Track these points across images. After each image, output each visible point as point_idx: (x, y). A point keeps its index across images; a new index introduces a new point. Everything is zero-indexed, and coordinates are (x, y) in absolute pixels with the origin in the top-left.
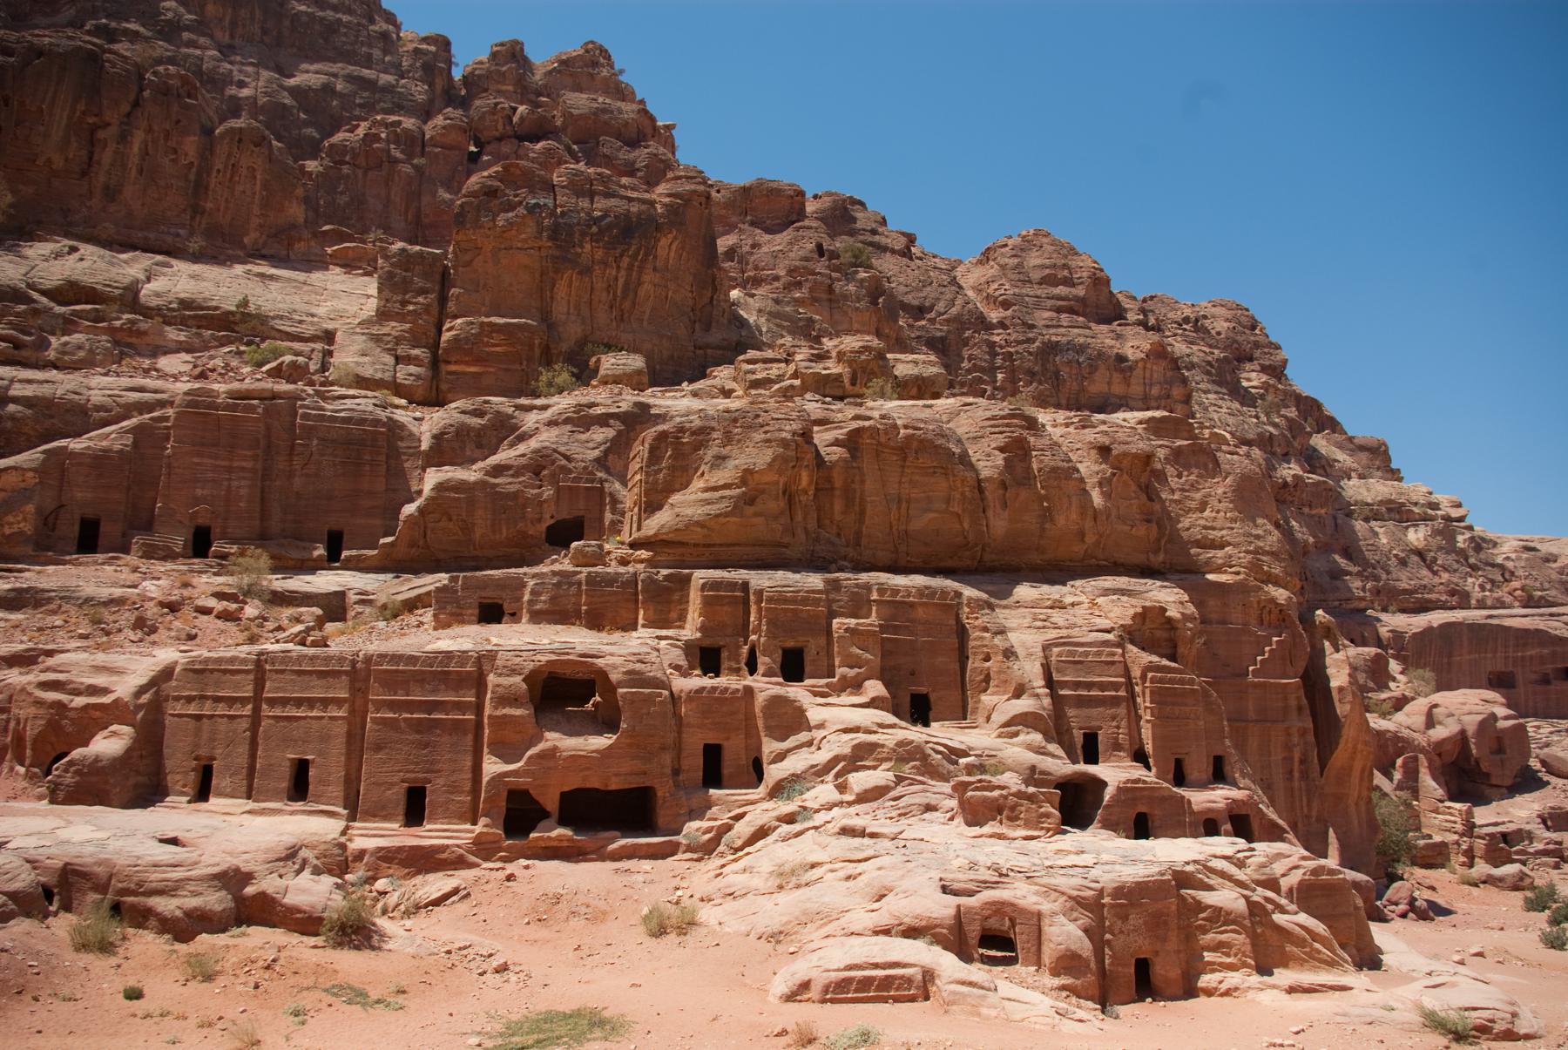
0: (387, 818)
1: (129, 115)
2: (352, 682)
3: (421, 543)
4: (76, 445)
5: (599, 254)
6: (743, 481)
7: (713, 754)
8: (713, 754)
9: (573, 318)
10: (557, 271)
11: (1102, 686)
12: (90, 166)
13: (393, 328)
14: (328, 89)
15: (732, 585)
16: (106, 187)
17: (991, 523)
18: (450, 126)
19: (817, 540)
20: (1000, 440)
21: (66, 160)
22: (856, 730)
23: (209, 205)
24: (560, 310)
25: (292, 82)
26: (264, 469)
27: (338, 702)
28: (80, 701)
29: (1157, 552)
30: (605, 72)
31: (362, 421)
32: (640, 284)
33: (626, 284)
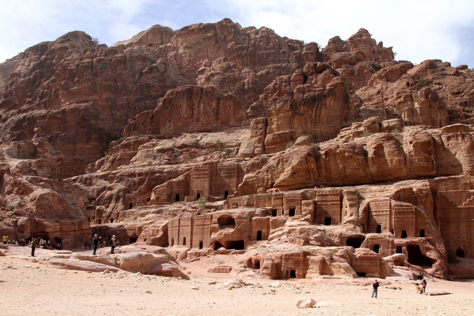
7: (259, 233)
8: (259, 233)
9: (300, 128)
13: (254, 140)
22: (292, 226)
31: (231, 166)
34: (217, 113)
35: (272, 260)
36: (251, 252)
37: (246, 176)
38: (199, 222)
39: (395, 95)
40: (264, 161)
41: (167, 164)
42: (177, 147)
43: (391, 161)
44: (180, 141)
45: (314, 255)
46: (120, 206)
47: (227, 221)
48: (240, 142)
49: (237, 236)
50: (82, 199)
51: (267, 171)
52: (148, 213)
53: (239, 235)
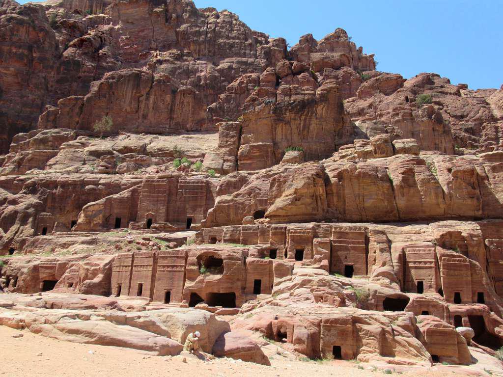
0: (160, 301)
2: (154, 260)
3: (215, 221)
4: (115, 196)
5: (293, 116)
6: (295, 192)
7: (258, 283)
8: (258, 283)
10: (277, 124)
11: (425, 263)
12: (138, 109)
13: (223, 150)
14: (230, 68)
15: (281, 228)
16: (143, 115)
17: (397, 202)
18: (269, 74)
19: (328, 212)
20: (402, 170)
21: (131, 108)
22: (306, 275)
23: (175, 116)
24: (279, 138)
25: (218, 67)
26: (168, 200)
27: (151, 265)
28: (93, 268)
29: (478, 210)
30: (343, 39)
31: (198, 182)
32: (310, 124)
33: (304, 125)
40: (243, 181)
42: (118, 151)
46: (28, 229)
47: (212, 263)
48: (204, 152)
49: (225, 285)
51: (249, 194)
53: (229, 285)
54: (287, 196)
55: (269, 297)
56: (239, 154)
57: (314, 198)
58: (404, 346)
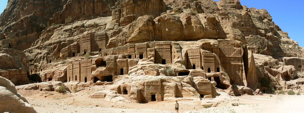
1: (84, 3)
6: (139, 29)
8: (122, 70)
15: (133, 45)
22: (143, 64)
31: (102, 34)
34: (94, 10)
35: (137, 87)
36: (119, 81)
37: (110, 39)
38: (84, 65)
39: (182, 3)
40: (120, 31)
41: (68, 37)
43: (196, 27)
44: (75, 25)
45: (169, 82)
48: (106, 23)
50: (25, 59)
51: (123, 35)
52: (58, 64)
54: (136, 32)
55: (127, 76)
56: (120, 22)
57: (148, 32)
58: (187, 92)
